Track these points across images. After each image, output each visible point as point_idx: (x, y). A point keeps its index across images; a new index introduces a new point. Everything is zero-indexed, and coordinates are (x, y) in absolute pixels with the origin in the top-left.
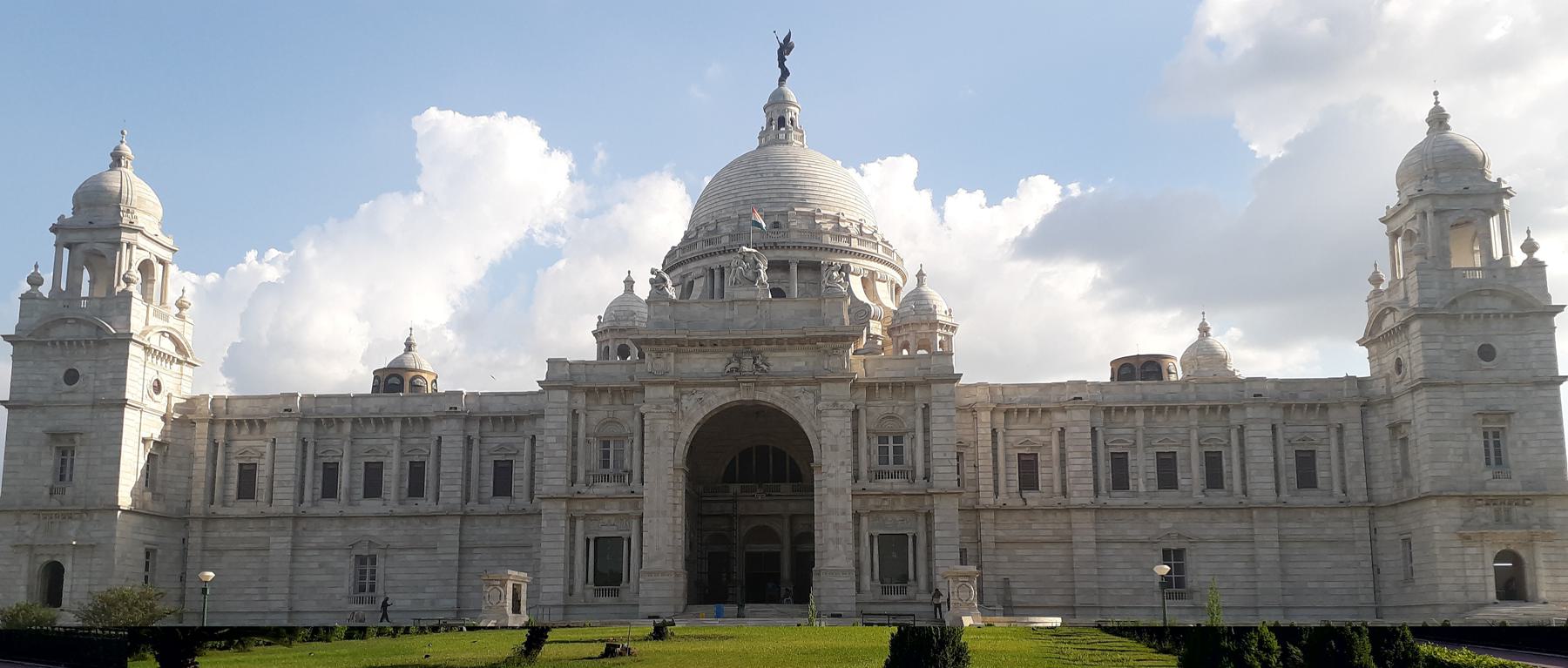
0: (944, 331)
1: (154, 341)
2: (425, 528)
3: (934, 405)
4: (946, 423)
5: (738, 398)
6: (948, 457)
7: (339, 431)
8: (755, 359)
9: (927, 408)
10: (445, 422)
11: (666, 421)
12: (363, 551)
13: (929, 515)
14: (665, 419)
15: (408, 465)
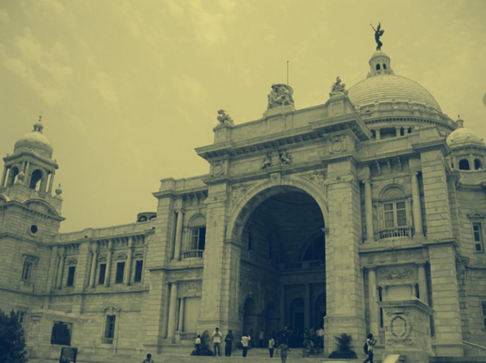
0: (477, 152)
1: (32, 207)
2: (138, 299)
3: (424, 170)
4: (436, 182)
5: (270, 185)
6: (440, 210)
7: (107, 247)
8: (281, 155)
9: (420, 175)
10: (149, 236)
11: (220, 208)
12: (110, 313)
13: (427, 266)
14: (219, 207)
15: (135, 264)
